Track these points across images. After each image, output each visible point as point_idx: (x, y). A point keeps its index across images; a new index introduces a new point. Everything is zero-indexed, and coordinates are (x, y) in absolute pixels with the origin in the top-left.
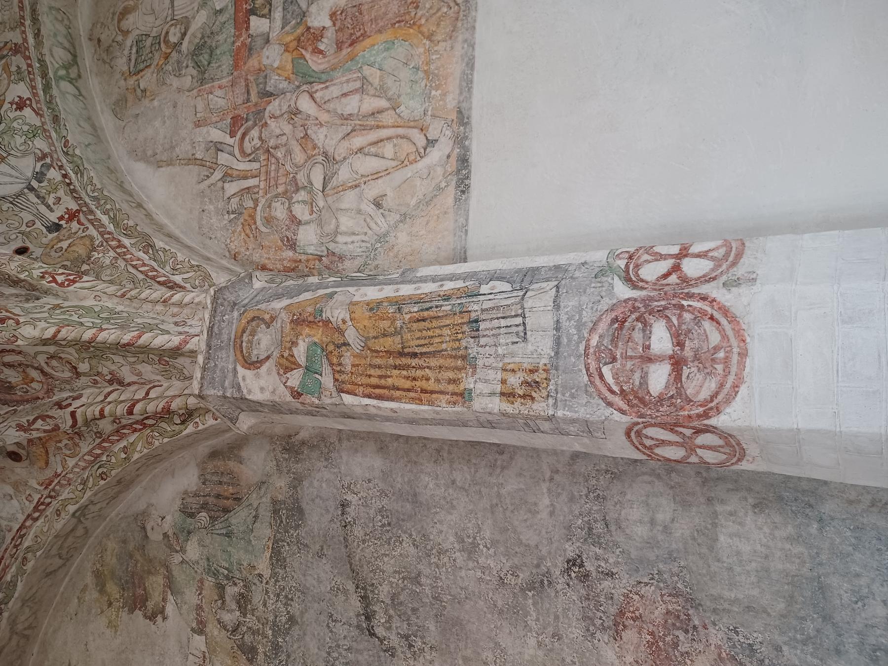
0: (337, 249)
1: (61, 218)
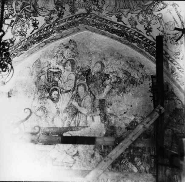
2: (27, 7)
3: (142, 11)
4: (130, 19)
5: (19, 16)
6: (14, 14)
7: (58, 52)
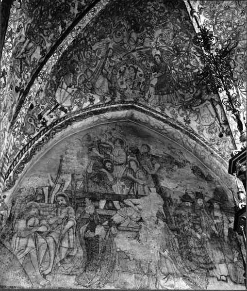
0: (14, 238)
1: (44, 119)
6: (76, 86)
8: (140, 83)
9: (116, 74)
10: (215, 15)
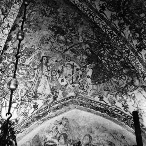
2: (30, 93)
3: (118, 93)
4: (109, 99)
5: (23, 100)
6: (19, 100)
7: (53, 128)
8: (78, 77)
9: (56, 75)
10: (121, 5)
